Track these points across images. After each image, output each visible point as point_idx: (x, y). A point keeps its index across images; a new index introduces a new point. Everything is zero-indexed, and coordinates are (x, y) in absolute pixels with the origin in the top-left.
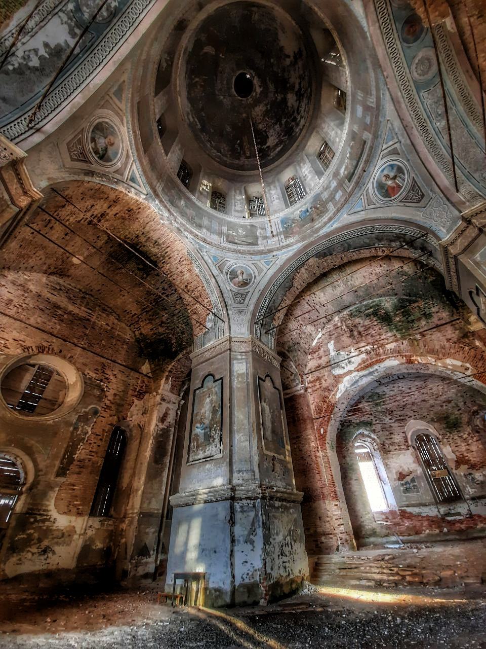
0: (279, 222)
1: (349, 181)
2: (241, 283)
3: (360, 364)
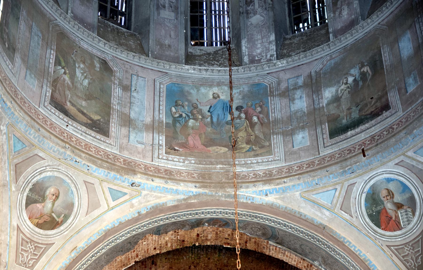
0: (164, 88)
1: (333, 134)
2: (46, 218)
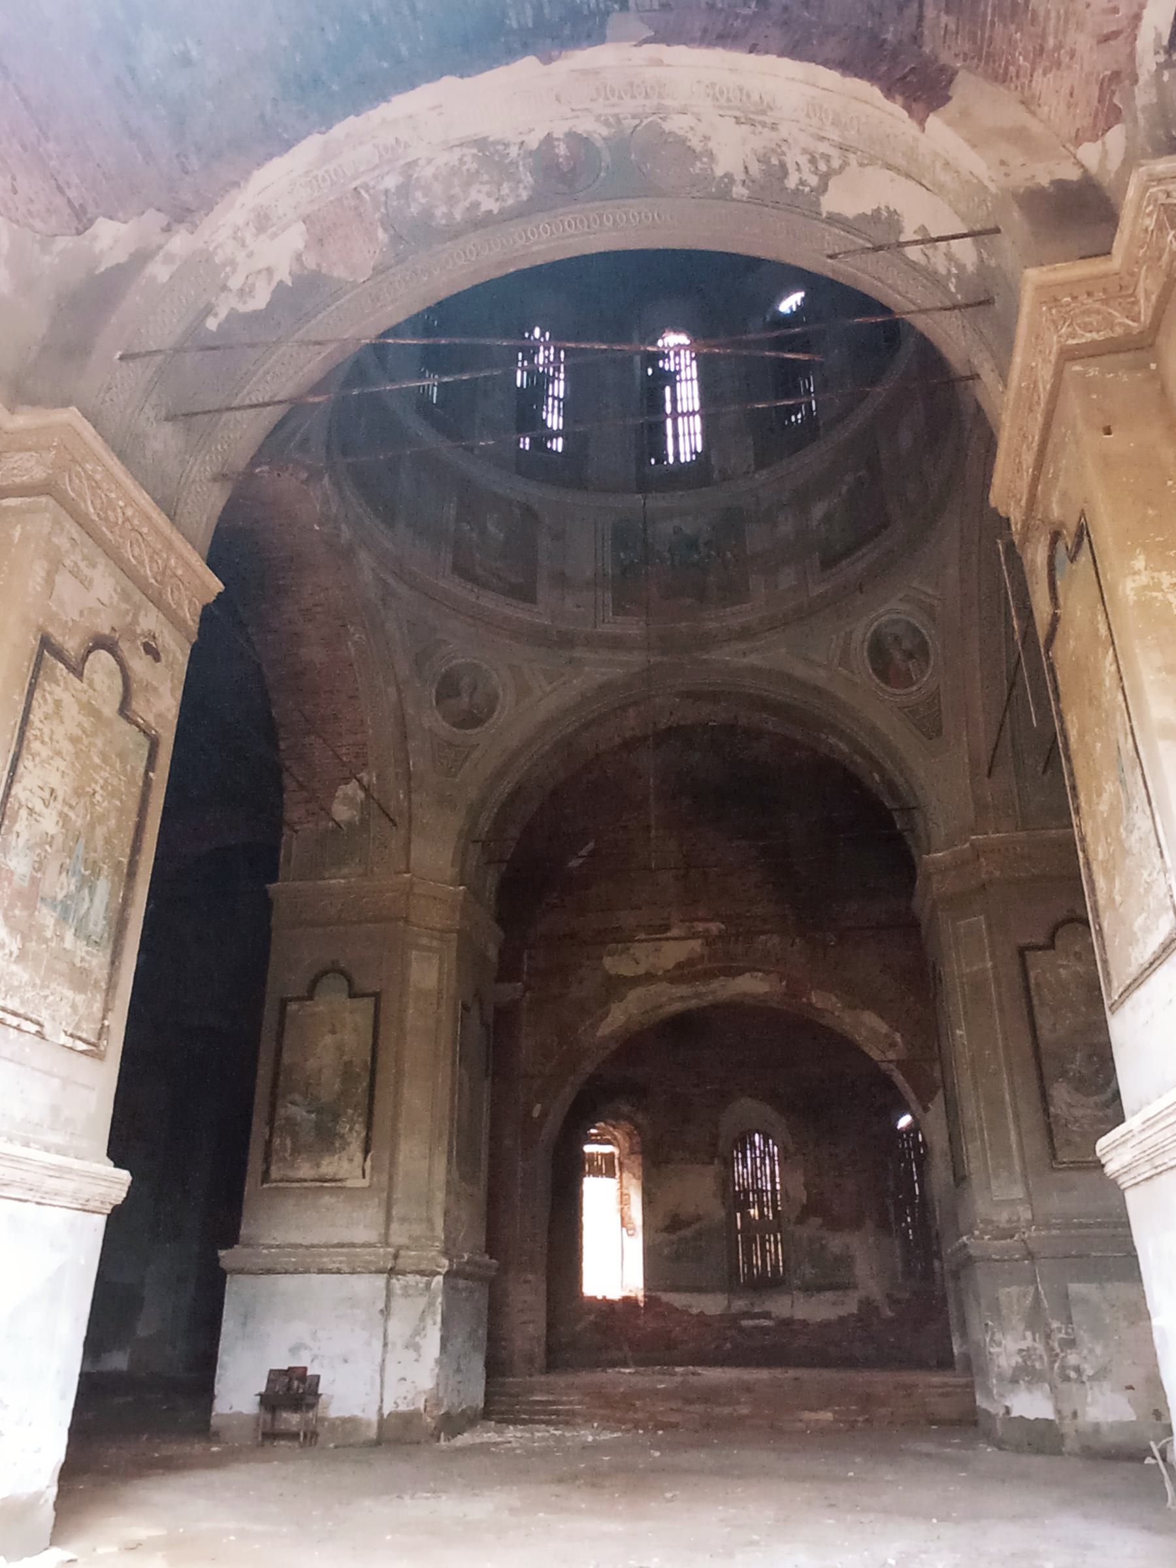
3: (679, 966)
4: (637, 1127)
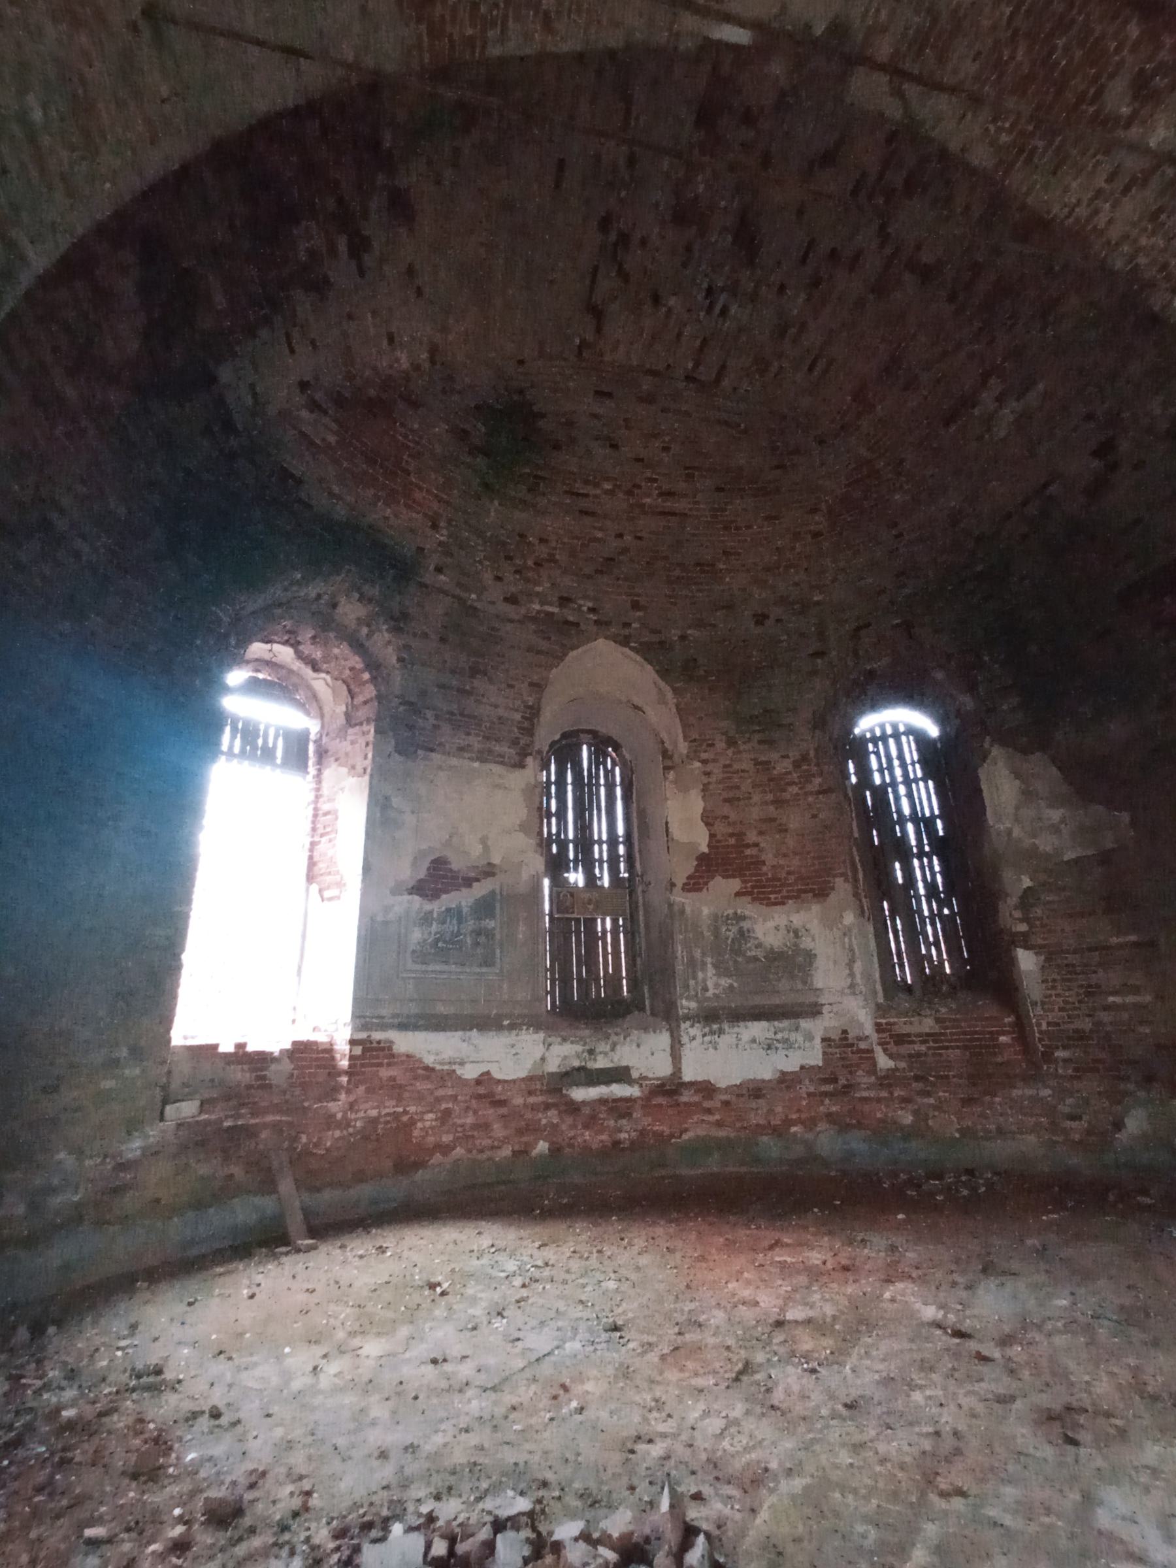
4: (374, 665)
